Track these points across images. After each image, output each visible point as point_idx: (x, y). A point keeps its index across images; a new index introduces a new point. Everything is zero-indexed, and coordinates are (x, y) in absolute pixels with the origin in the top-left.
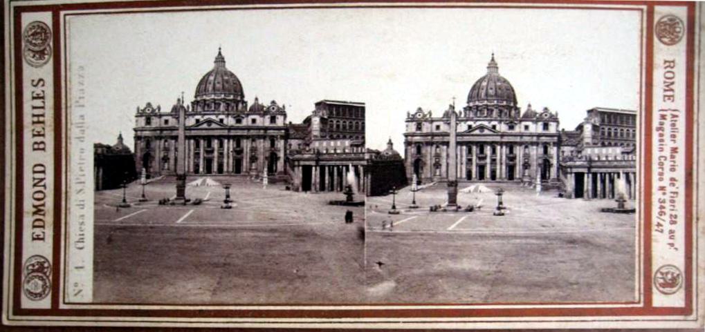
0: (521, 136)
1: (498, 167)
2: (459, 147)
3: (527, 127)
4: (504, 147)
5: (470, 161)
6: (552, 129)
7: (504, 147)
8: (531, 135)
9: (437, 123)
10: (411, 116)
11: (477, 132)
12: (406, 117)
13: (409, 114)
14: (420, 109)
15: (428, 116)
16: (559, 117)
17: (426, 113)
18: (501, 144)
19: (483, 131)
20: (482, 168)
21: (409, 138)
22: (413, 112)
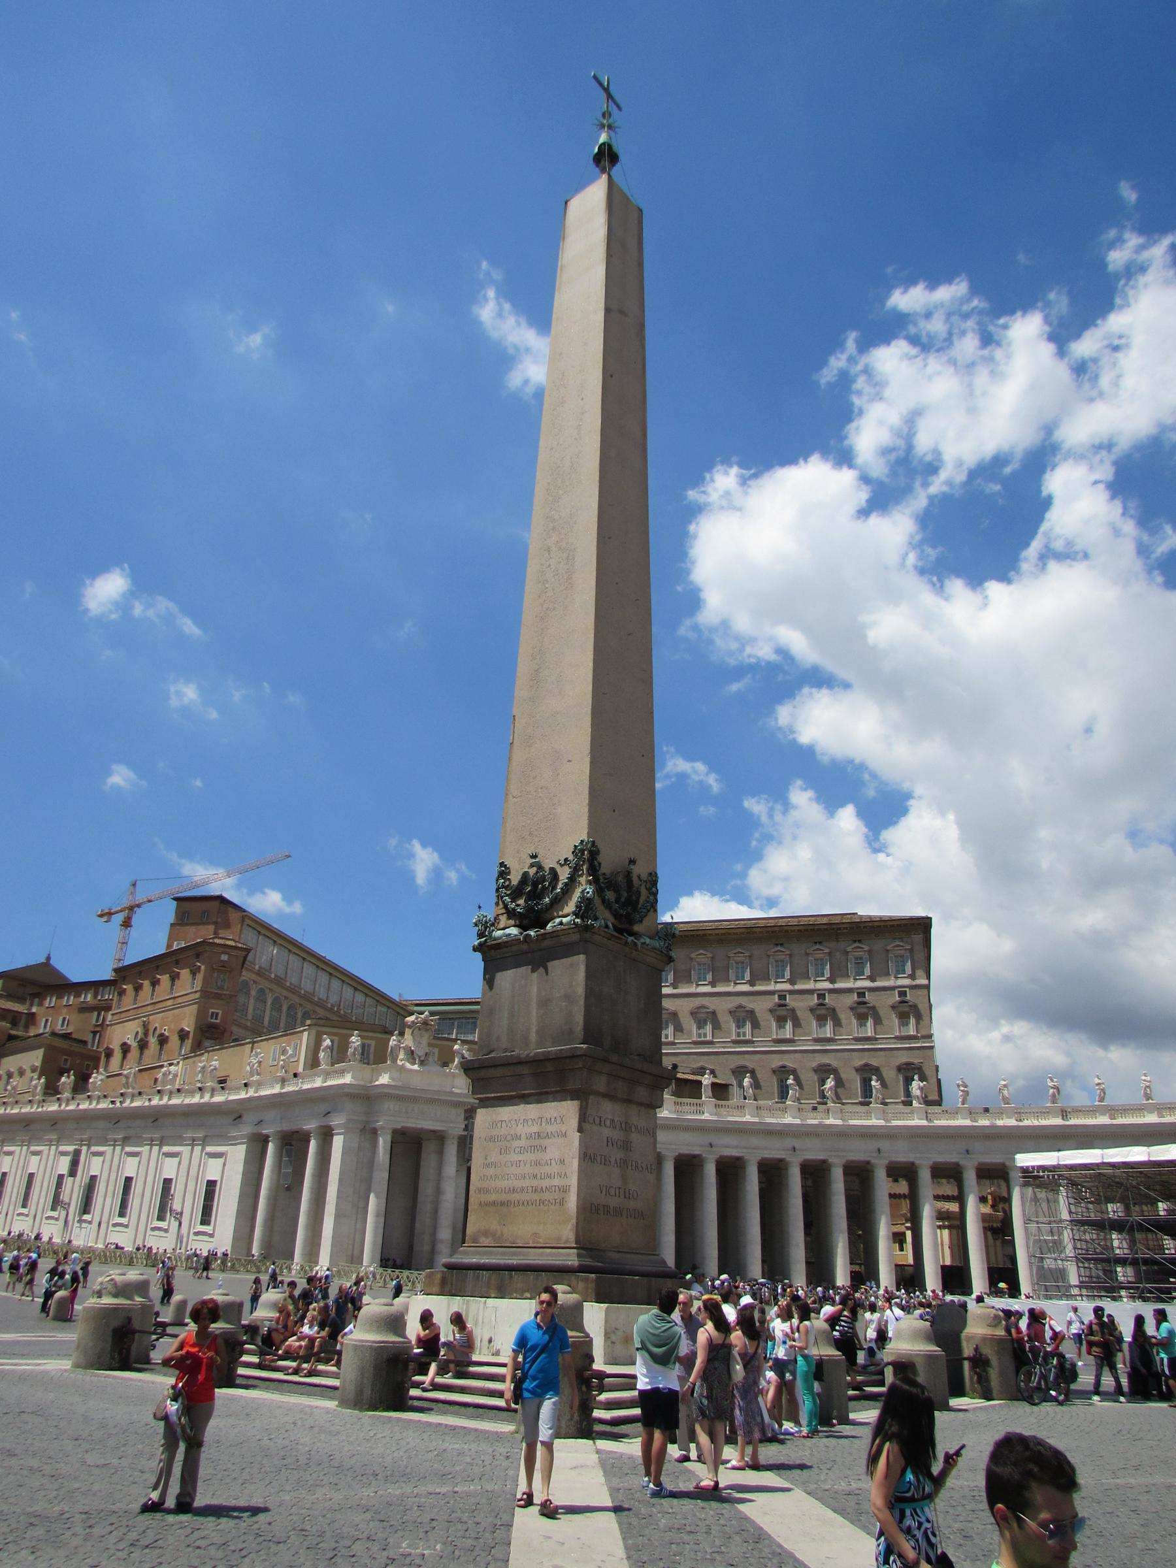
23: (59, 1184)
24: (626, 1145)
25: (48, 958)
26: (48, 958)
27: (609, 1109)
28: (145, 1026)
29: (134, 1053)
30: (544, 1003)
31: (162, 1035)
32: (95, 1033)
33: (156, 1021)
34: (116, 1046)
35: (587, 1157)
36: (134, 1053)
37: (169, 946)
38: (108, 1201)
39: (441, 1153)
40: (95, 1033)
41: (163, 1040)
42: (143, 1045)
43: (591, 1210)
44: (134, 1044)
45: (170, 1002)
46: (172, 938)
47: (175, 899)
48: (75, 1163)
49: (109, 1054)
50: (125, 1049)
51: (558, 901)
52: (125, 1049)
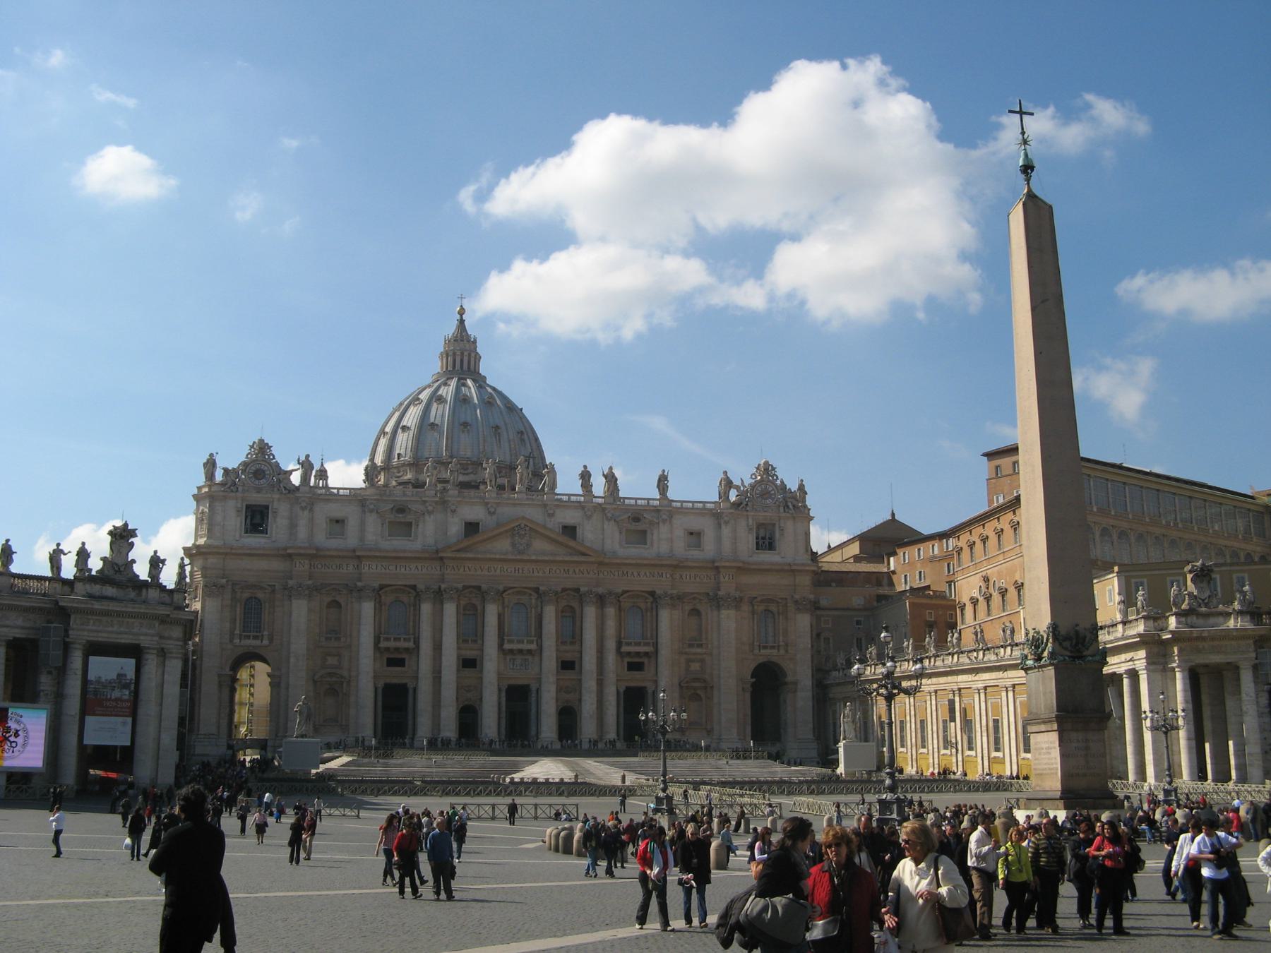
0: (678, 566)
1: (590, 684)
2: (426, 608)
3: (695, 536)
4: (611, 611)
5: (469, 663)
6: (786, 552)
7: (611, 611)
8: (714, 567)
9: (336, 511)
10: (219, 476)
11: (503, 545)
12: (201, 479)
13: (210, 465)
14: (262, 449)
15: (296, 479)
16: (810, 501)
17: (289, 463)
18: (601, 600)
19: (529, 545)
20: (518, 700)
21: (212, 560)
22: (232, 457)
23: (945, 729)
24: (1087, 748)
25: (893, 515)
26: (893, 515)
27: (1074, 735)
28: (986, 580)
29: (982, 605)
30: (1045, 694)
31: (1000, 588)
32: (949, 583)
33: (992, 573)
34: (965, 599)
35: (1063, 756)
36: (982, 605)
37: (990, 501)
38: (985, 739)
39: (1238, 679)
40: (949, 583)
41: (1003, 592)
42: (988, 599)
43: (1066, 776)
44: (981, 599)
45: (1001, 557)
46: (992, 492)
47: (984, 455)
48: (952, 710)
49: (963, 608)
50: (975, 602)
51: (1043, 650)
52: (975, 602)
